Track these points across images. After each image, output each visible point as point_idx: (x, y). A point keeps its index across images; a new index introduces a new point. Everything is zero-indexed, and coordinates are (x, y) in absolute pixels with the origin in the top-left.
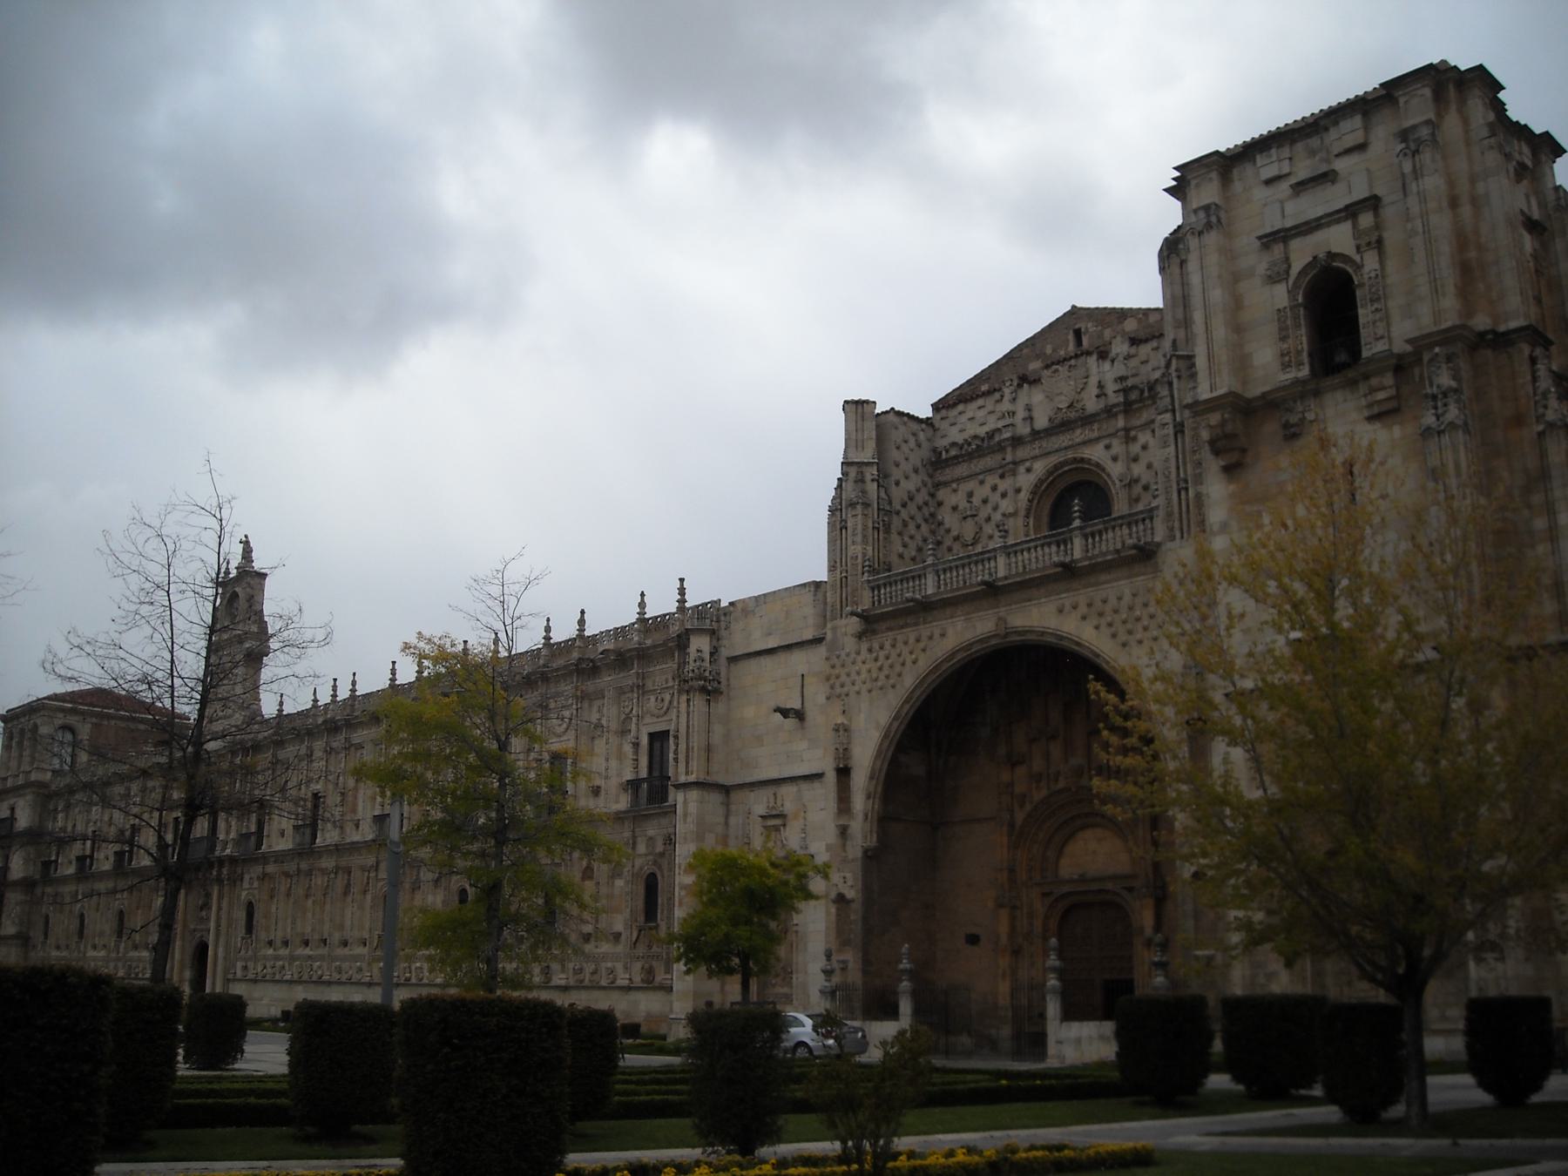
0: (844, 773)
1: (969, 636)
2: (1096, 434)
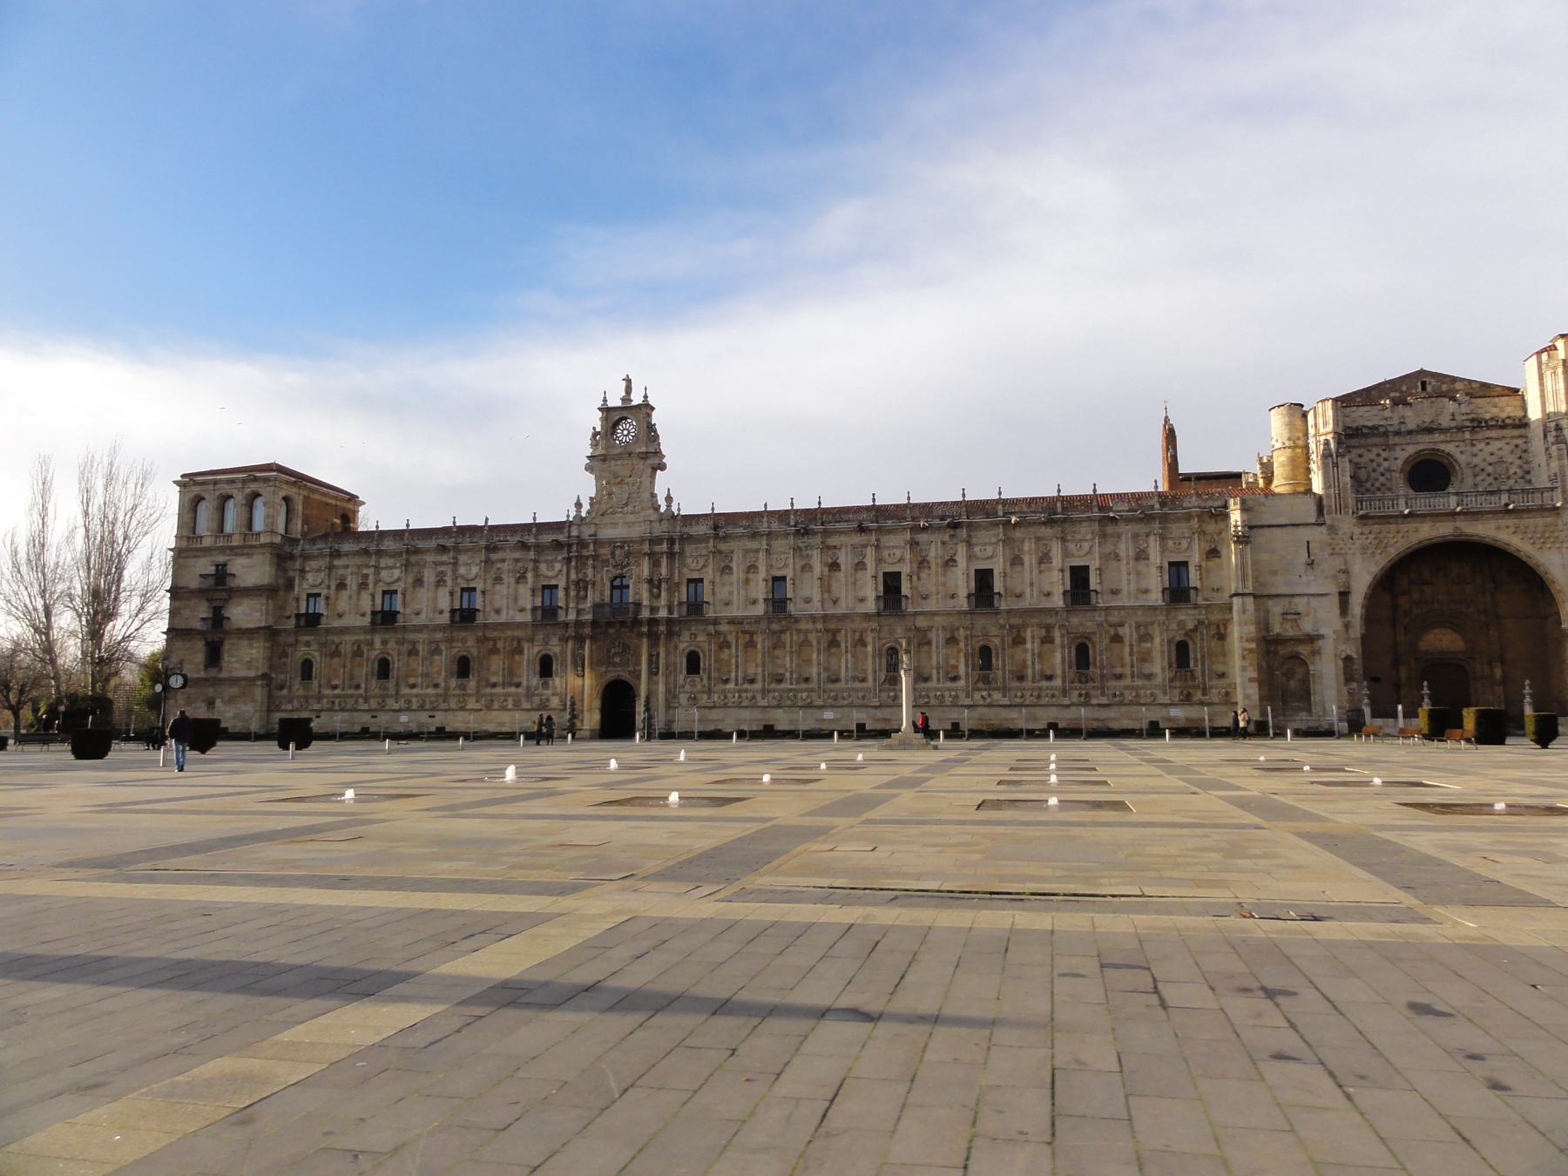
0: (1344, 596)
1: (1434, 533)
2: (1448, 439)
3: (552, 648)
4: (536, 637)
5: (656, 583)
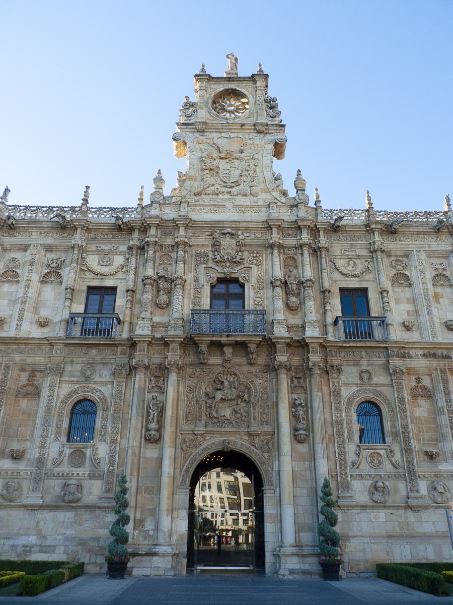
3: (98, 387)
4: (68, 368)
5: (294, 287)
